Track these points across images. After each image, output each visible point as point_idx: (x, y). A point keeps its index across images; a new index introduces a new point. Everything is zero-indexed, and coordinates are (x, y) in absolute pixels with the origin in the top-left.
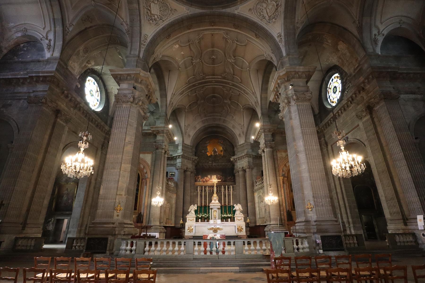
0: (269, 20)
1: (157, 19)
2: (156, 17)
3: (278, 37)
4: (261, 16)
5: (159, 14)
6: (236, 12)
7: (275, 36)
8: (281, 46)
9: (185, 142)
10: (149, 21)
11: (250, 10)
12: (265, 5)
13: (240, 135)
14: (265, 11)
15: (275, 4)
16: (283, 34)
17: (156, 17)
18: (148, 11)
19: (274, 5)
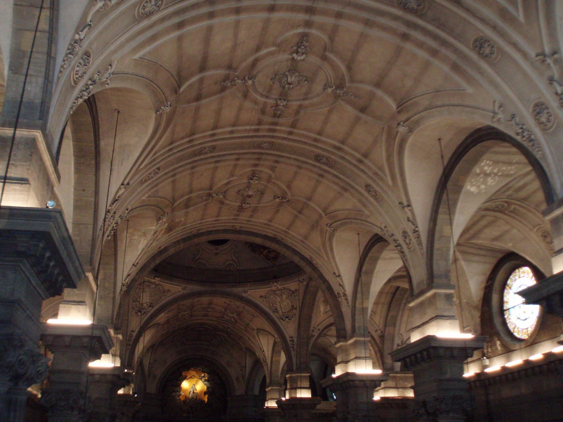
0: (283, 315)
1: (146, 307)
2: (145, 305)
3: (290, 341)
4: (274, 308)
5: (148, 301)
6: (244, 295)
7: (288, 339)
8: (293, 355)
9: (148, 391)
10: (137, 313)
11: (261, 296)
12: (279, 299)
13: (237, 379)
14: (278, 304)
15: (290, 304)
16: (295, 340)
17: (145, 305)
18: (138, 303)
19: (288, 304)
